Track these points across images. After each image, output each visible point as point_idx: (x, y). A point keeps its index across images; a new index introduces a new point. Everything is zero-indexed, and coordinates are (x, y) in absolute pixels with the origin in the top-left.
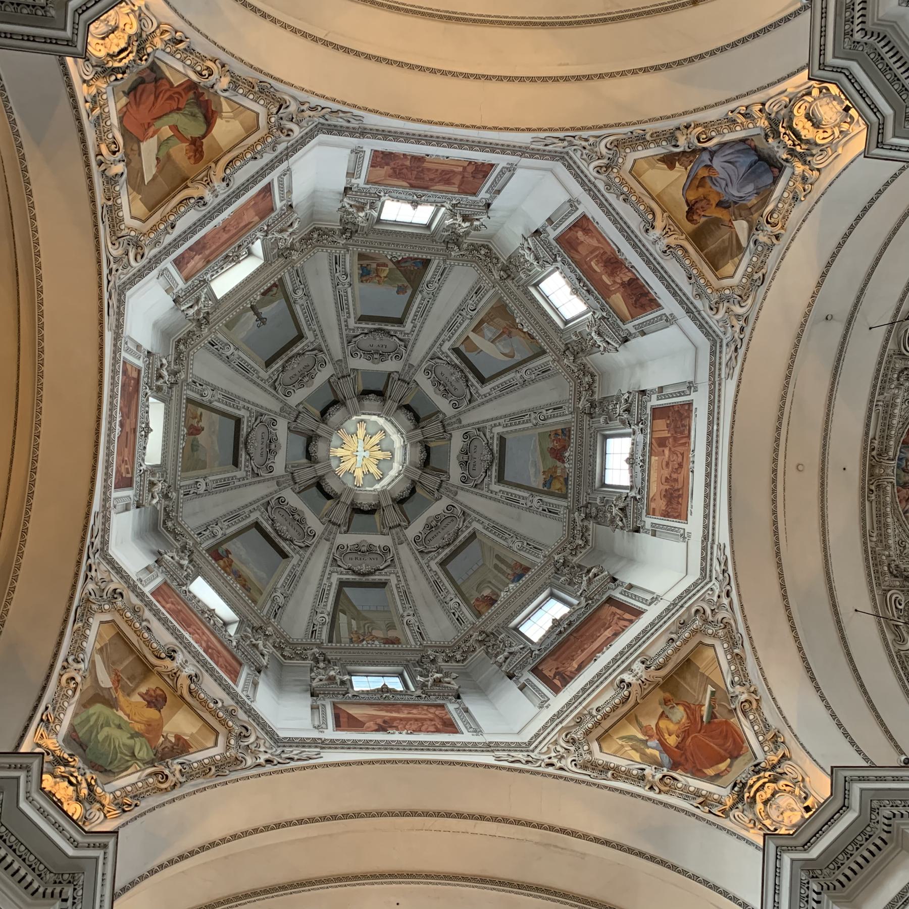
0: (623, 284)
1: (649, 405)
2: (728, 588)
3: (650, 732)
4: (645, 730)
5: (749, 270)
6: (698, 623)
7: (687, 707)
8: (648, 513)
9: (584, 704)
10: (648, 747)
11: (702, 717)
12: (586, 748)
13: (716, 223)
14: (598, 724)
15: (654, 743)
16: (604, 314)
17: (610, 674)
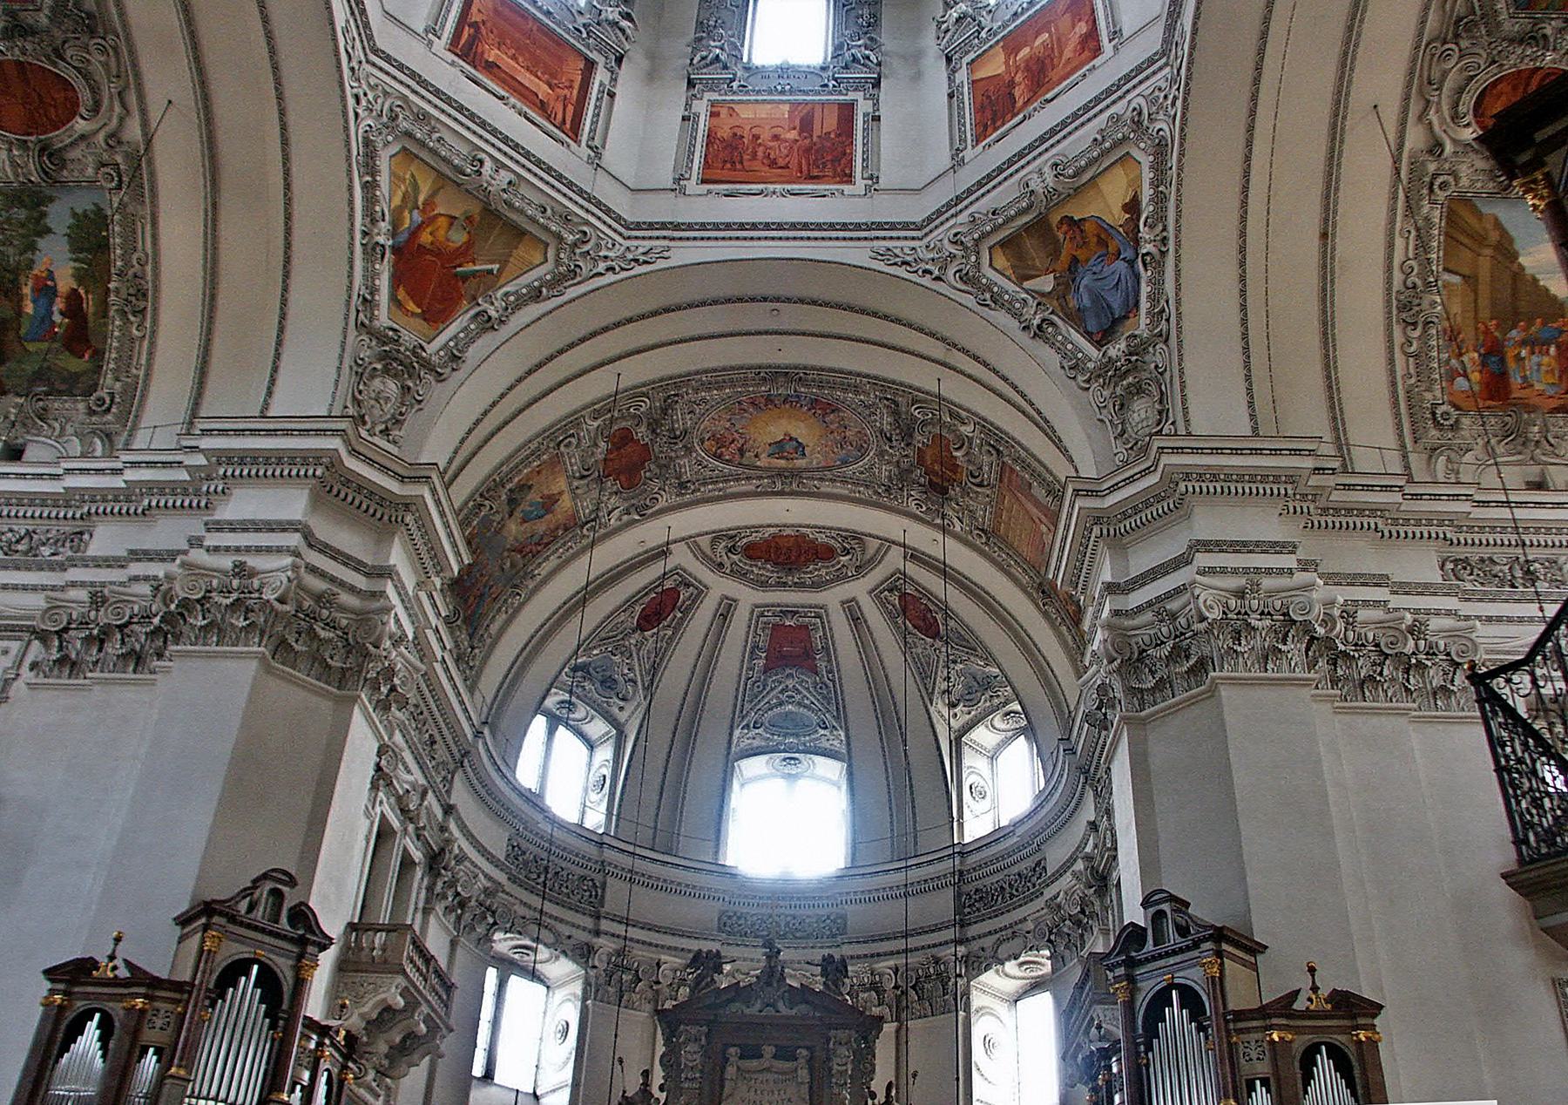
0: (1012, 84)
1: (859, 96)
2: (617, 269)
3: (428, 208)
4: (429, 203)
5: (996, 289)
6: (571, 238)
7: (469, 245)
8: (713, 103)
9: (443, 118)
10: (411, 212)
11: (460, 266)
12: (390, 138)
13: (1055, 254)
14: (423, 144)
15: (417, 217)
16: (983, 34)
17: (487, 141)
